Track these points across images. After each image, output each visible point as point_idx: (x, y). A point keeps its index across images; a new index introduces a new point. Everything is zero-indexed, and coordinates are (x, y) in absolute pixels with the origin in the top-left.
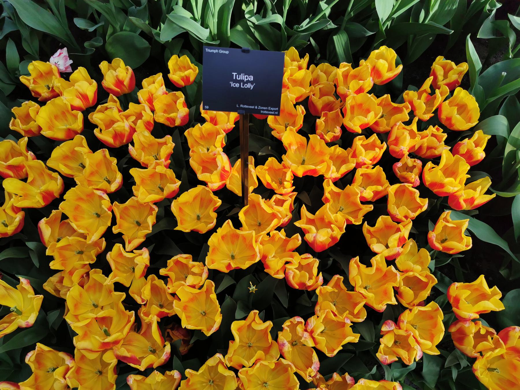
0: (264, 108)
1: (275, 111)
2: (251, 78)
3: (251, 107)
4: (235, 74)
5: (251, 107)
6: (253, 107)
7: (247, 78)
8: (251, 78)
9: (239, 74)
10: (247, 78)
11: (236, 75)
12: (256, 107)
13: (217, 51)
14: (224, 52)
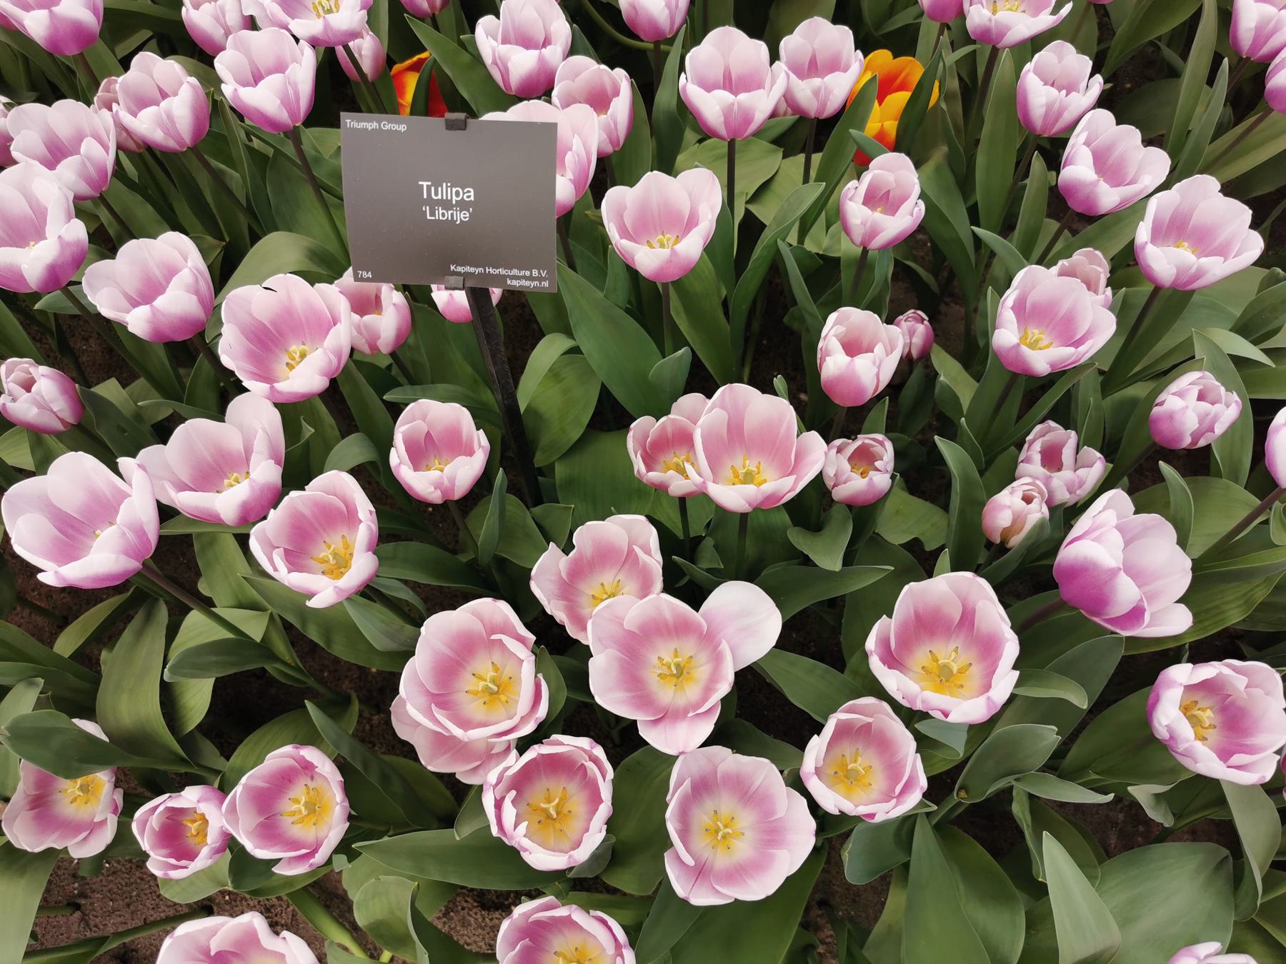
1: (540, 279)
2: (470, 195)
4: (425, 184)
7: (457, 194)
8: (470, 195)
9: (437, 184)
10: (457, 194)
11: (429, 188)
13: (375, 125)
14: (395, 127)
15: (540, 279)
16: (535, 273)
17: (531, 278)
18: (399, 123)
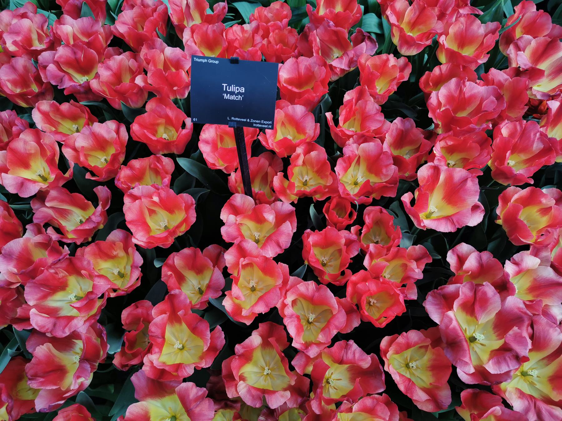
0: (257, 121)
2: (243, 90)
3: (242, 120)
4: (225, 85)
5: (242, 120)
6: (245, 120)
7: (238, 89)
8: (243, 90)
9: (230, 85)
10: (238, 89)
12: (248, 120)
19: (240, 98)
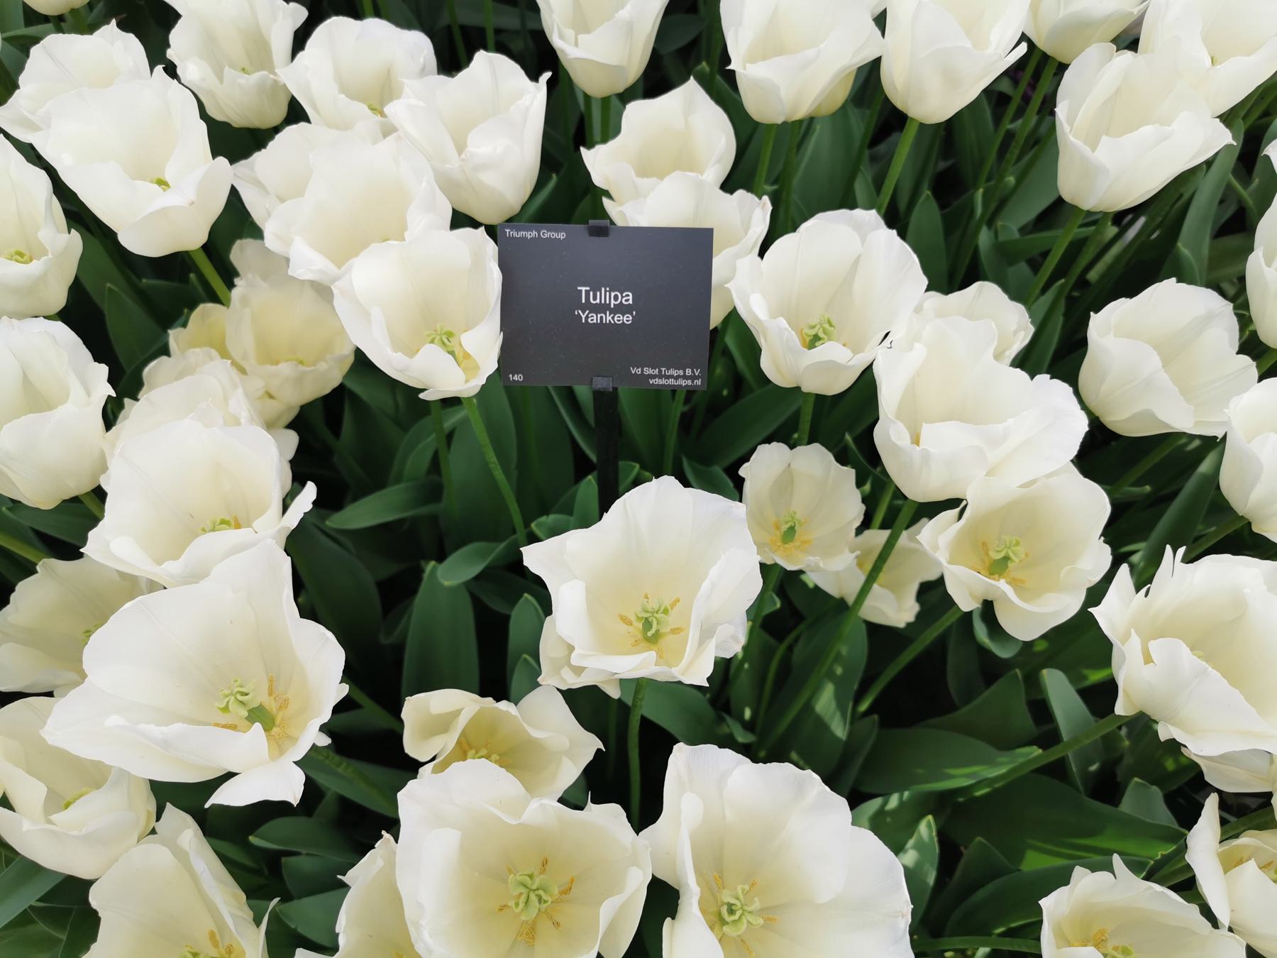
2: (628, 298)
4: (584, 289)
7: (616, 298)
8: (628, 298)
9: (595, 289)
10: (616, 298)
11: (587, 293)
13: (534, 233)
15: (693, 378)
16: (689, 372)
17: (685, 377)
18: (557, 231)
19: (627, 319)
